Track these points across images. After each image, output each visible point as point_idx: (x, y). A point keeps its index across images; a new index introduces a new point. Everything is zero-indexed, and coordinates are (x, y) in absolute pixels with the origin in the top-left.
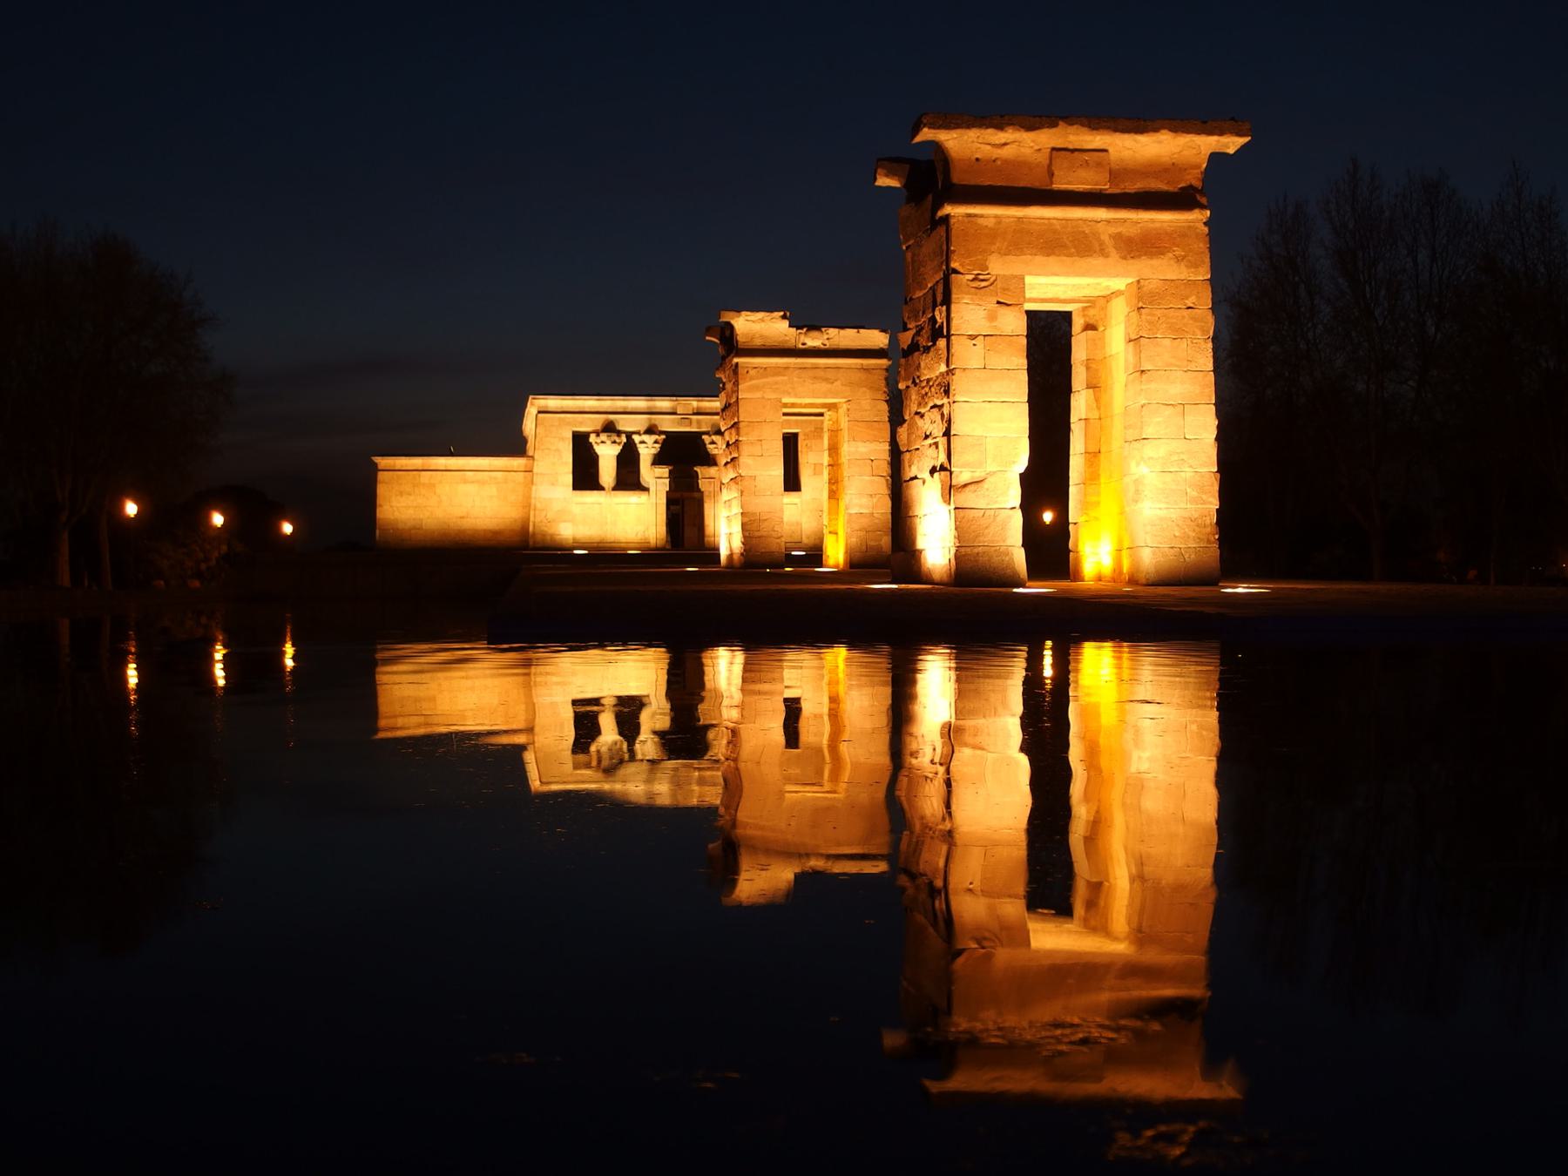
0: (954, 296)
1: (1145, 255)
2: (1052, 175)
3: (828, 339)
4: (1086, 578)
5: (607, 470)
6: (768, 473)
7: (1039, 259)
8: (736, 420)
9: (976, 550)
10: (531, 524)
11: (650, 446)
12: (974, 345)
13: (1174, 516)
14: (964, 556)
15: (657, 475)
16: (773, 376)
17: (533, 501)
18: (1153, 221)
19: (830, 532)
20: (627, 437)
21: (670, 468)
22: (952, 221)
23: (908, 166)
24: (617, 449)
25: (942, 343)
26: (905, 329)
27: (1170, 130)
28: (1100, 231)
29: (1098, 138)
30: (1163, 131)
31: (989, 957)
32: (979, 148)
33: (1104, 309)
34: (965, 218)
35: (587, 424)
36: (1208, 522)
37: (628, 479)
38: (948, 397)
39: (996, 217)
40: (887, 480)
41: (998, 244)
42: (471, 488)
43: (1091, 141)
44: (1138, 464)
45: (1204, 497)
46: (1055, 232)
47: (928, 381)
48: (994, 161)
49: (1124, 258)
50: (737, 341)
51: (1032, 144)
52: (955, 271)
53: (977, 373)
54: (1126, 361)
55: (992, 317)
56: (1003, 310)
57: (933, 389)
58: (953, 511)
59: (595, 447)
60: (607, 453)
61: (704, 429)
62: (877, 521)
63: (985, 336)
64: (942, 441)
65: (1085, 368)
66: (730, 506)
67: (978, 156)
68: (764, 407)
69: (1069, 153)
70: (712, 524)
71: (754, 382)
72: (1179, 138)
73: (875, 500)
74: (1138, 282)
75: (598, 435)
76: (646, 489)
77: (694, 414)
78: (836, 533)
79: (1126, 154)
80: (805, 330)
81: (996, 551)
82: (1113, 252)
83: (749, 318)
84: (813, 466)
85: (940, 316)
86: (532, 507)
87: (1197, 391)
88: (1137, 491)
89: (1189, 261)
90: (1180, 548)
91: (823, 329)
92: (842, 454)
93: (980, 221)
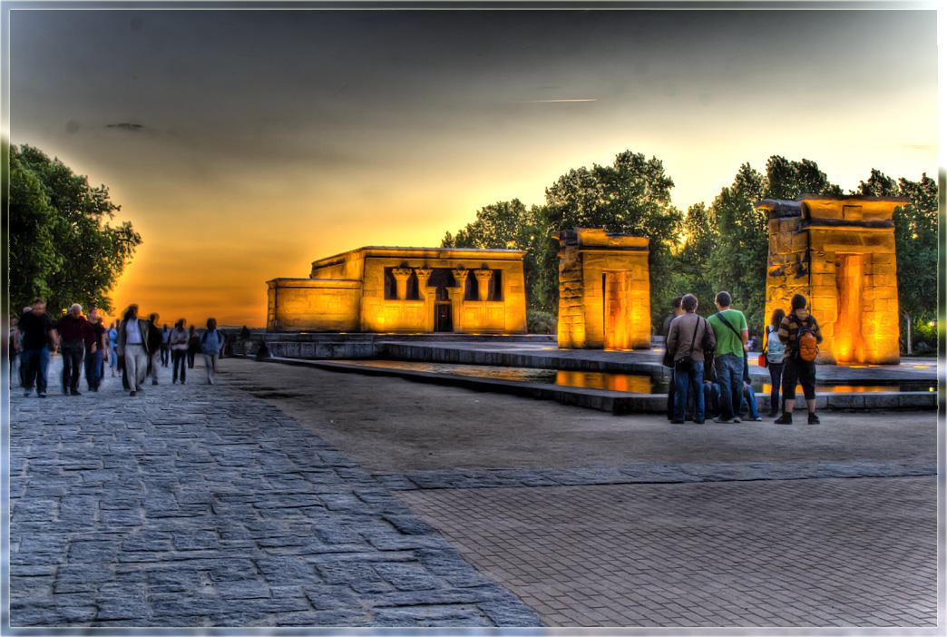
2: (844, 215)
5: (402, 289)
26: (772, 265)
35: (392, 263)
37: (413, 294)
42: (328, 298)
47: (792, 288)
55: (825, 266)
56: (828, 264)
60: (402, 280)
61: (454, 267)
76: (423, 300)
78: (613, 332)
85: (805, 266)
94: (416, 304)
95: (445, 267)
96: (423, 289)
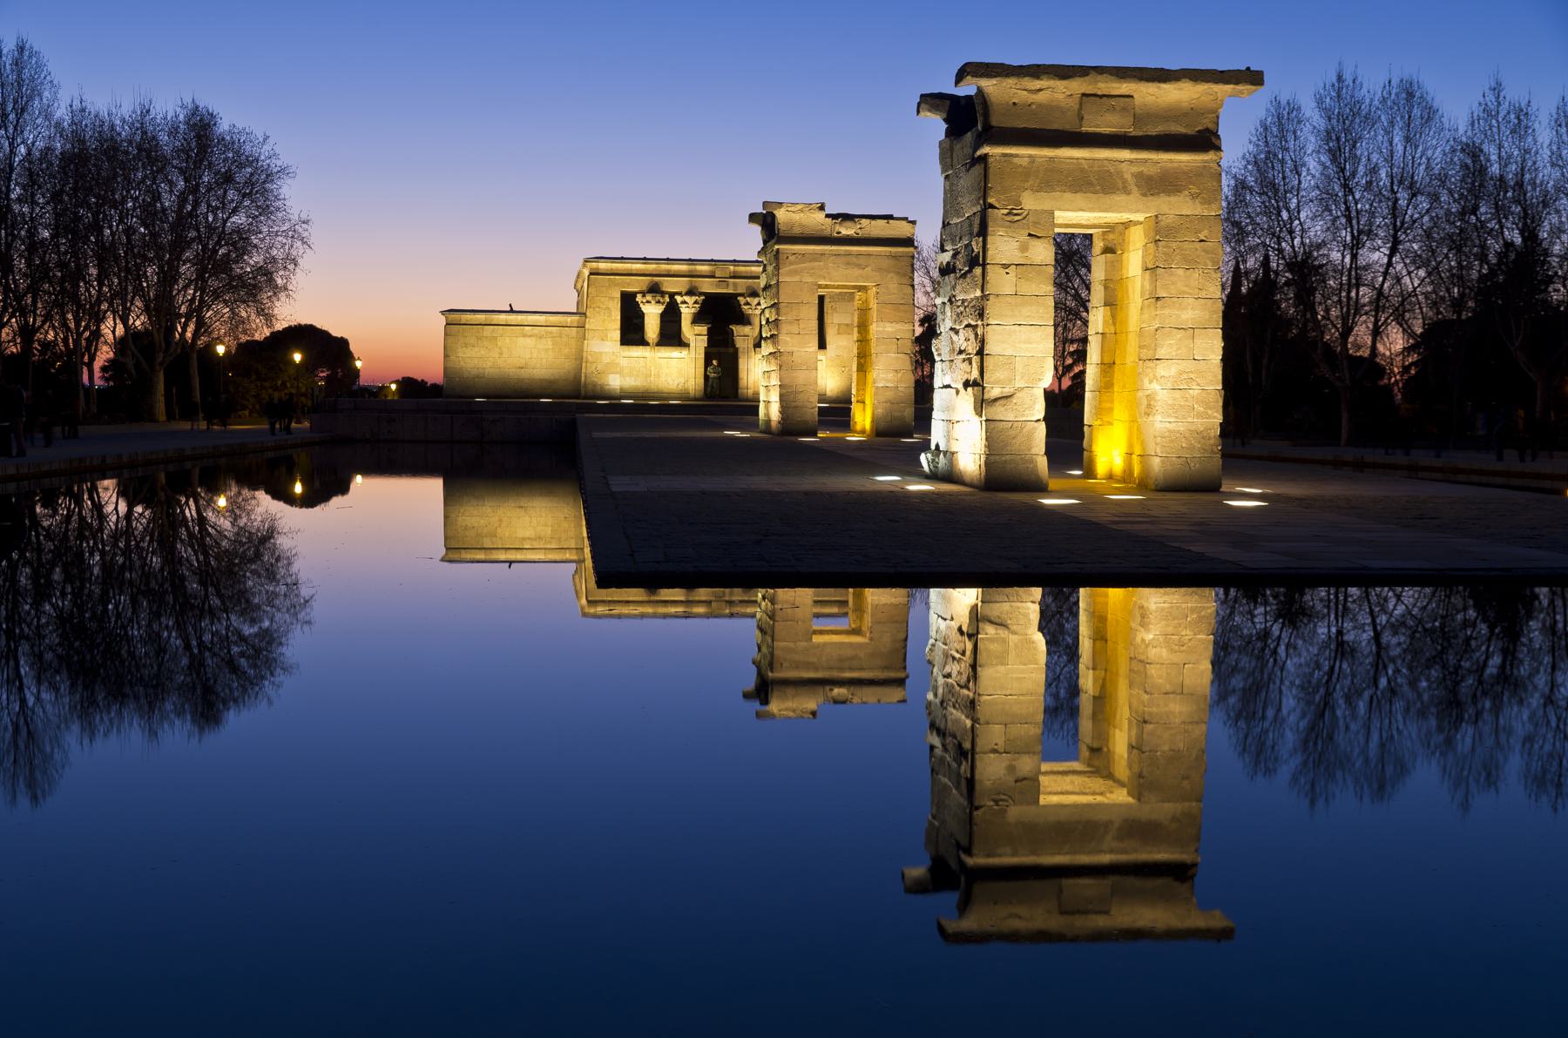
0: (990, 229)
1: (1164, 192)
3: (860, 228)
4: (1099, 476)
5: (652, 327)
6: (802, 350)
7: (1068, 195)
8: (776, 301)
9: (1004, 458)
10: (583, 375)
11: (691, 306)
12: (1007, 273)
13: (1182, 429)
14: (993, 463)
15: (696, 332)
16: (810, 261)
17: (585, 354)
18: (1171, 161)
19: (858, 401)
20: (669, 297)
21: (709, 326)
22: (991, 160)
23: (948, 102)
24: (660, 309)
25: (978, 271)
27: (1191, 80)
28: (1124, 170)
29: (1125, 85)
30: (1183, 80)
31: (1003, 812)
32: (1016, 93)
33: (1122, 234)
34: (1003, 159)
35: (634, 284)
36: (1212, 434)
37: (671, 336)
38: (982, 320)
39: (1030, 156)
40: (911, 357)
41: (1030, 183)
42: (528, 340)
43: (1119, 88)
44: (1151, 382)
45: (1210, 412)
46: (1082, 170)
47: (963, 301)
48: (1029, 105)
49: (1144, 195)
50: (779, 229)
51: (1064, 90)
52: (992, 206)
53: (1009, 299)
54: (1142, 286)
55: (1024, 248)
56: (1035, 242)
57: (967, 310)
58: (984, 423)
59: (641, 305)
60: (652, 312)
62: (901, 394)
63: (1016, 265)
64: (976, 360)
65: (1103, 288)
66: (769, 377)
67: (1014, 101)
68: (801, 290)
69: (1098, 99)
70: (745, 378)
71: (792, 267)
72: (1198, 86)
73: (899, 375)
74: (1156, 216)
75: (644, 296)
76: (687, 345)
77: (731, 277)
79: (1150, 99)
80: (840, 220)
81: (1022, 458)
82: (1135, 189)
83: (790, 209)
84: (837, 327)
85: (976, 247)
86: (584, 360)
87: (1207, 317)
88: (1149, 406)
89: (1203, 198)
90: (1187, 458)
91: (857, 220)
92: (871, 331)
93: (1016, 160)
94: (673, 354)
95: (724, 291)
96: (688, 330)
